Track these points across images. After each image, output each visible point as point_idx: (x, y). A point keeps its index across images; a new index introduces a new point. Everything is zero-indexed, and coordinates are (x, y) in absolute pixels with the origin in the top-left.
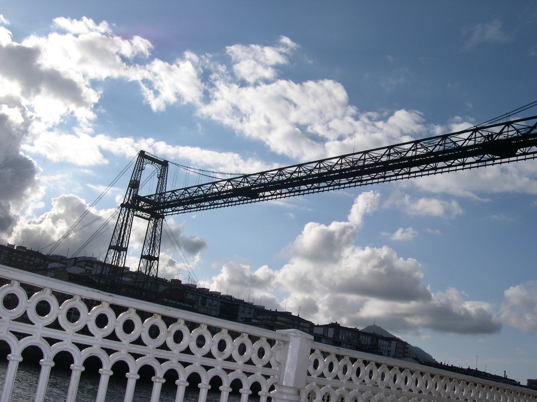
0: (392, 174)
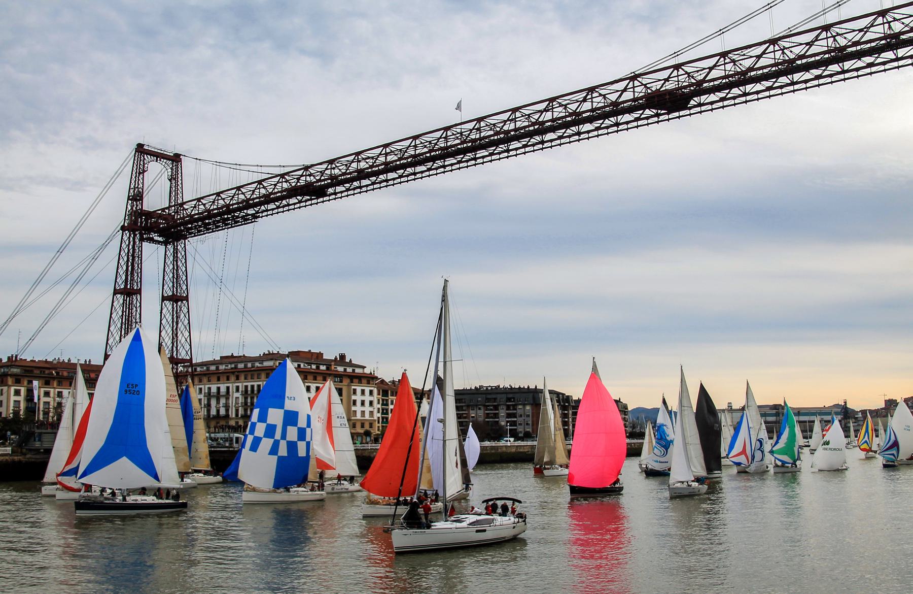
0: (519, 145)
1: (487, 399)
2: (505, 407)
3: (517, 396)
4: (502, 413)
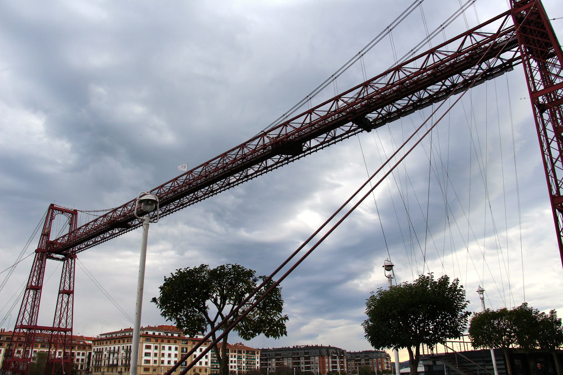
1: (293, 353)
3: (310, 351)
4: (302, 360)
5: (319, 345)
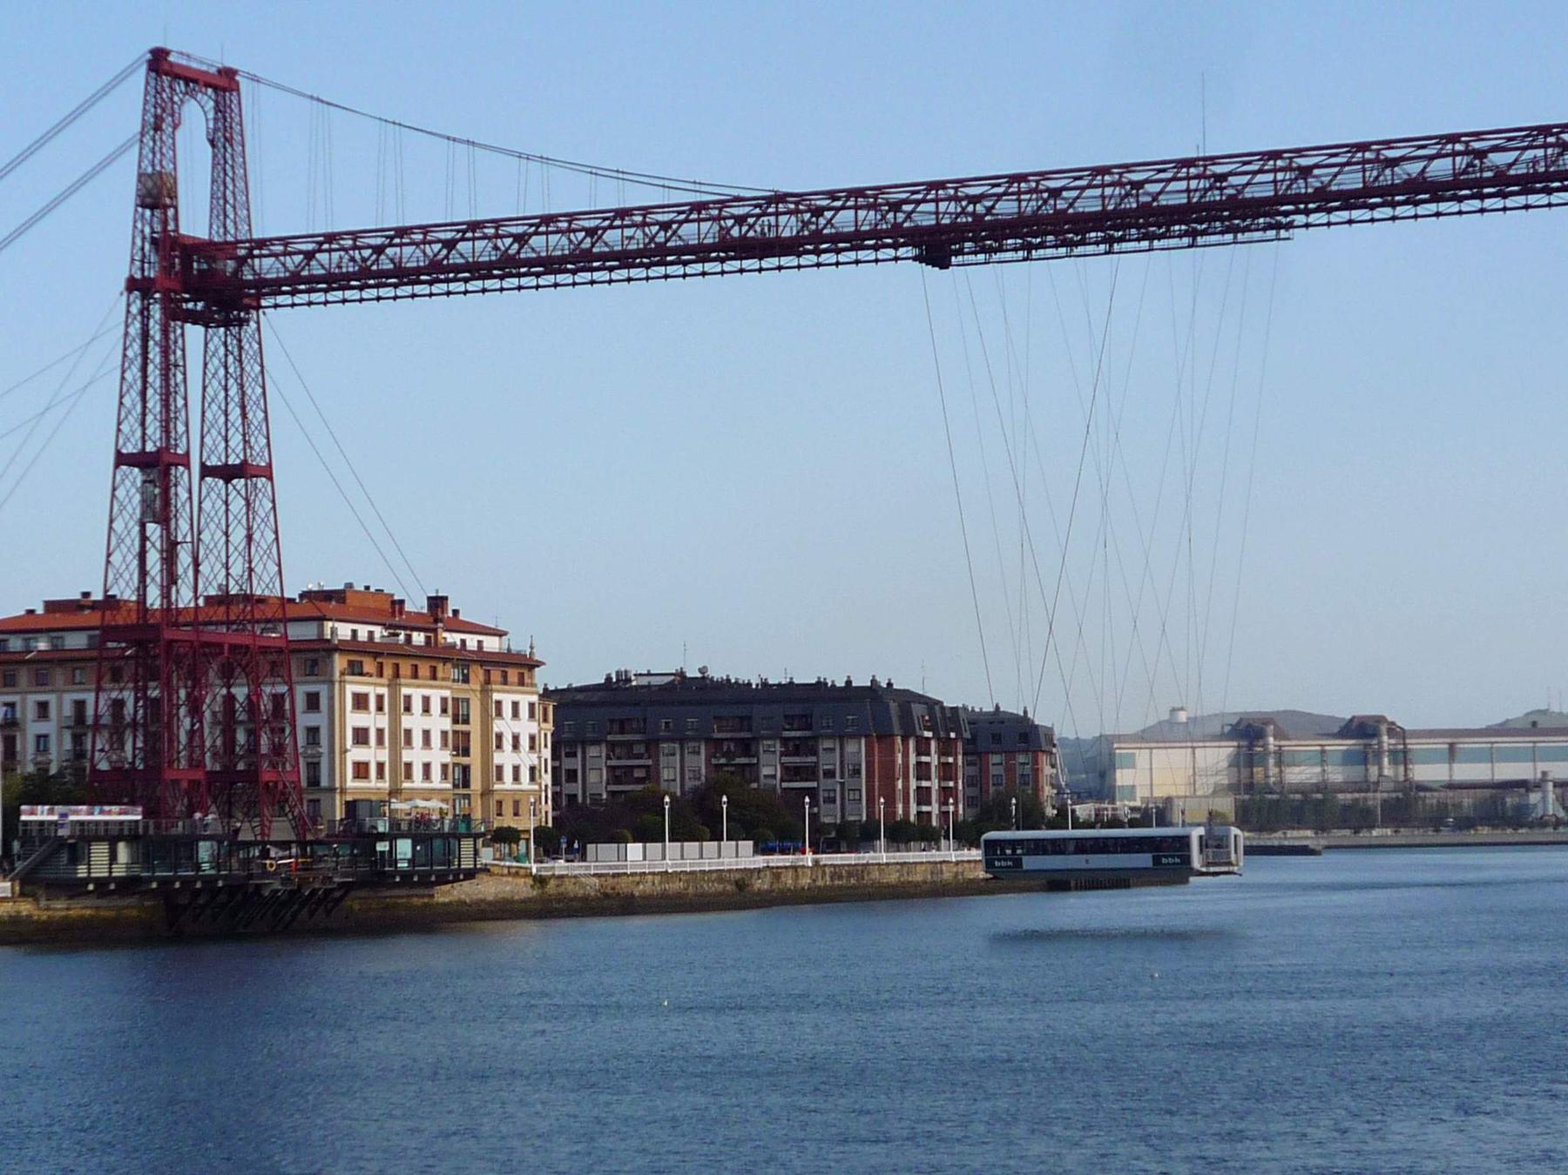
2: (778, 748)
5: (861, 681)
